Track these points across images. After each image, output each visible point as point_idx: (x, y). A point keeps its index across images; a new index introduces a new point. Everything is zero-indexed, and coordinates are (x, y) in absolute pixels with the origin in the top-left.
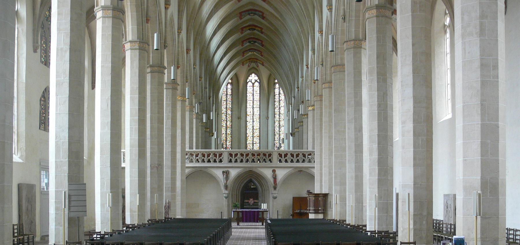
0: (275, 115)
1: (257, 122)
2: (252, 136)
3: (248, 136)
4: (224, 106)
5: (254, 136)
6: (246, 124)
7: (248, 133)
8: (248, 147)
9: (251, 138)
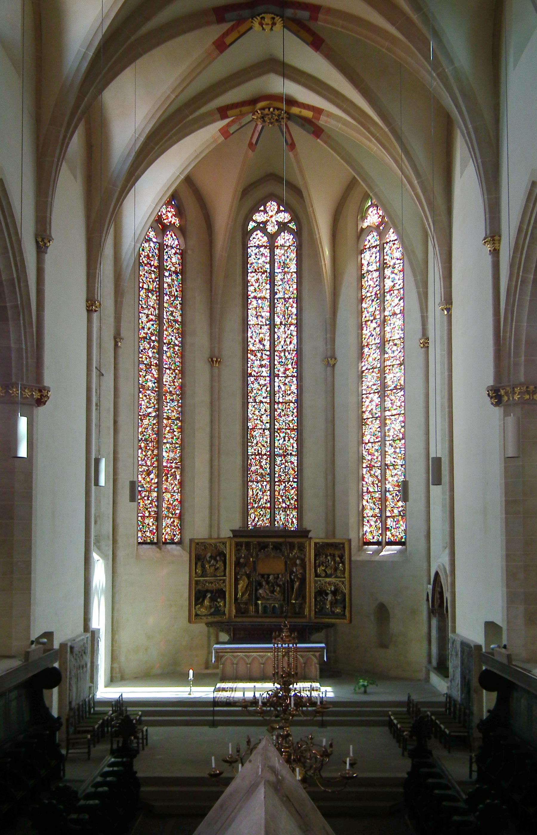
0: (362, 347)
1: (286, 377)
2: (268, 426)
3: (253, 429)
4: (146, 311)
5: (276, 427)
6: (246, 384)
7: (250, 416)
8: (253, 468)
9: (262, 435)
